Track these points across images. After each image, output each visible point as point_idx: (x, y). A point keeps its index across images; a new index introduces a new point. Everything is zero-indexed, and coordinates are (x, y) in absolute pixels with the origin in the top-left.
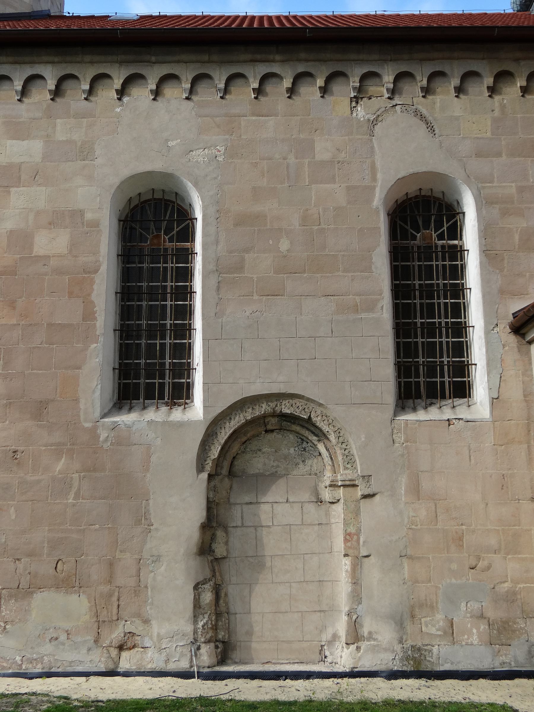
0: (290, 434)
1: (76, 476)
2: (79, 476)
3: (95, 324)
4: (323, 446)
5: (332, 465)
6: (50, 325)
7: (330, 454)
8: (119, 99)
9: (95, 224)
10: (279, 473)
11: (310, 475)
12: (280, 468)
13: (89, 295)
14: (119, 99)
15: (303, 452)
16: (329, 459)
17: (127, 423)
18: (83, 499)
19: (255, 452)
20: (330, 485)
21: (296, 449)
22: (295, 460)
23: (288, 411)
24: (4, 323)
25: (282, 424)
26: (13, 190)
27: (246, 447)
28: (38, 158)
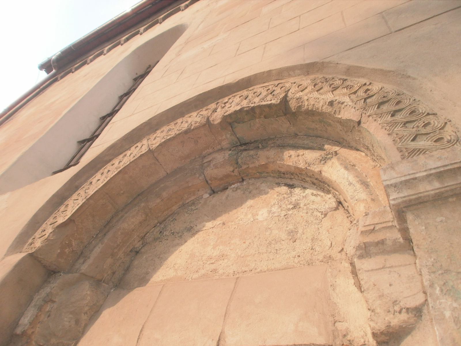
0: (261, 183)
5: (369, 200)
7: (358, 175)
10: (221, 272)
11: (310, 263)
12: (226, 261)
15: (290, 212)
16: (358, 186)
19: (180, 235)
20: (358, 248)
21: (275, 209)
22: (268, 233)
25: (240, 161)
27: (165, 226)
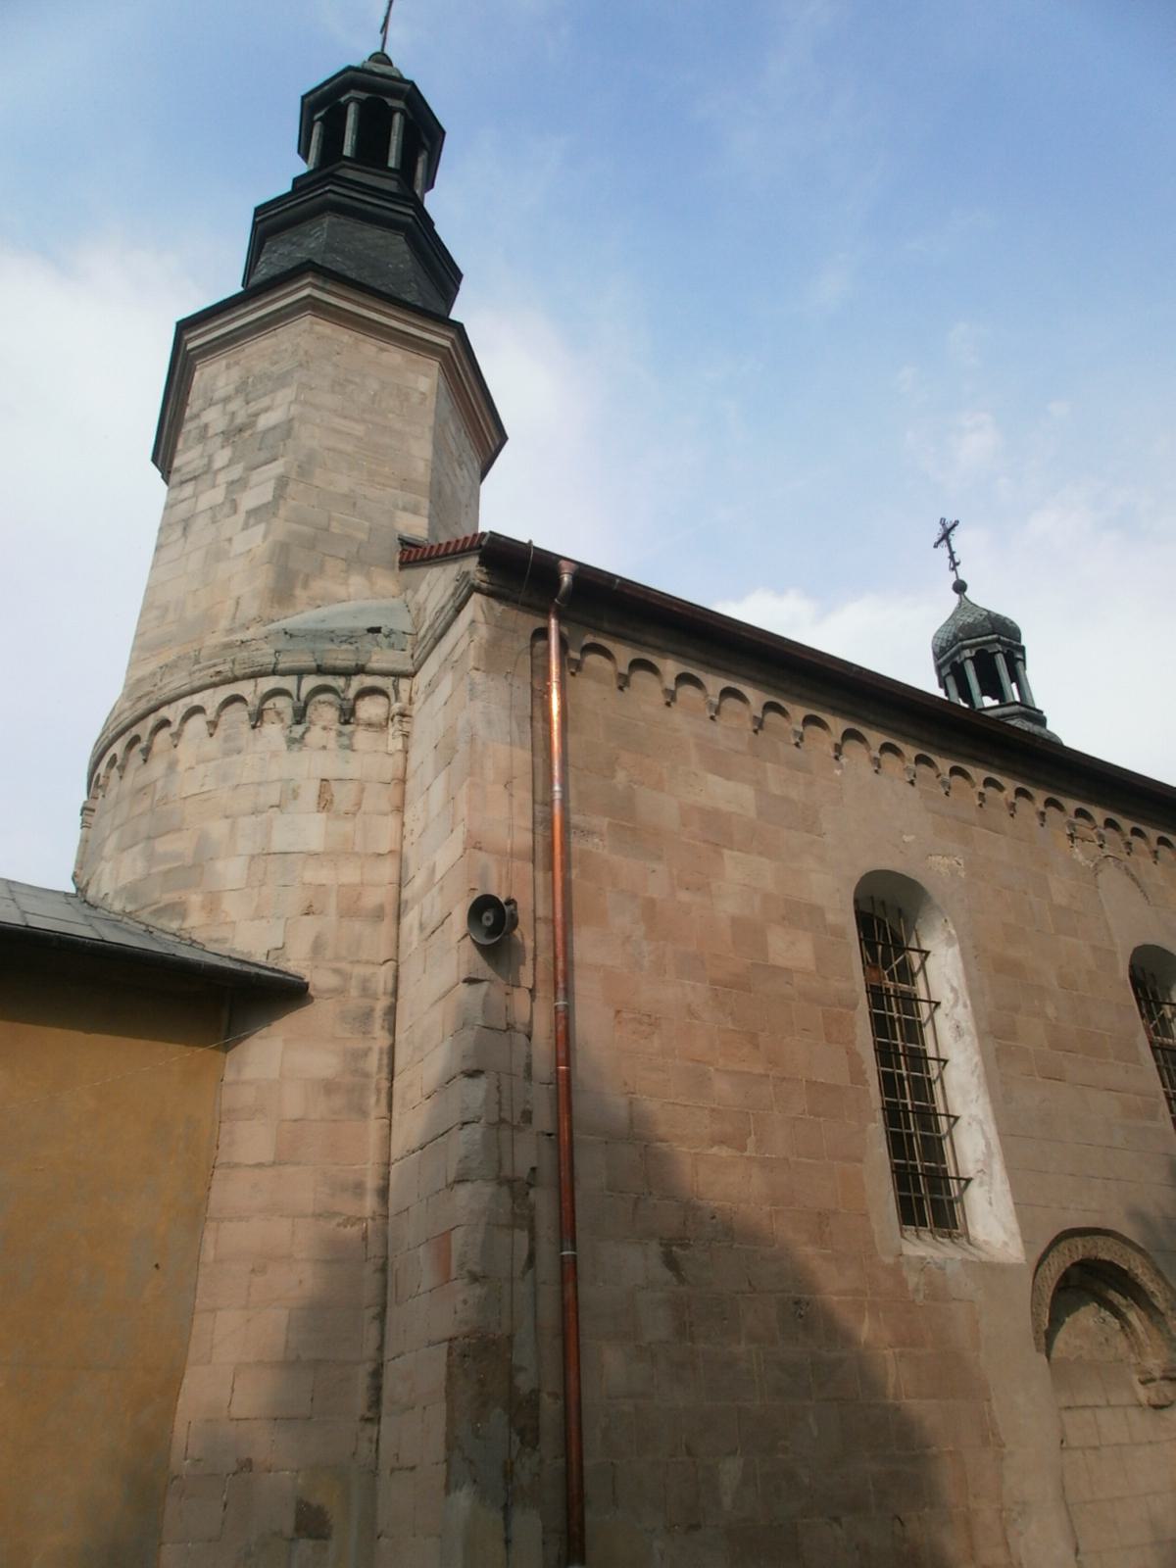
1: (889, 1352)
2: (894, 1353)
3: (868, 1091)
4: (1134, 1314)
6: (811, 1083)
8: (836, 758)
9: (838, 932)
13: (852, 1042)
14: (836, 758)
17: (938, 1261)
18: (907, 1397)
23: (1107, 1258)
24: (746, 1069)
26: (726, 852)
28: (752, 813)
